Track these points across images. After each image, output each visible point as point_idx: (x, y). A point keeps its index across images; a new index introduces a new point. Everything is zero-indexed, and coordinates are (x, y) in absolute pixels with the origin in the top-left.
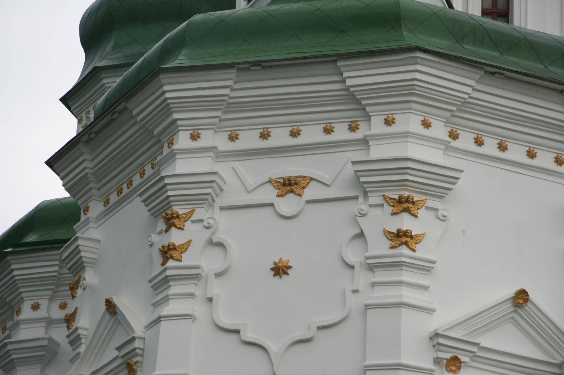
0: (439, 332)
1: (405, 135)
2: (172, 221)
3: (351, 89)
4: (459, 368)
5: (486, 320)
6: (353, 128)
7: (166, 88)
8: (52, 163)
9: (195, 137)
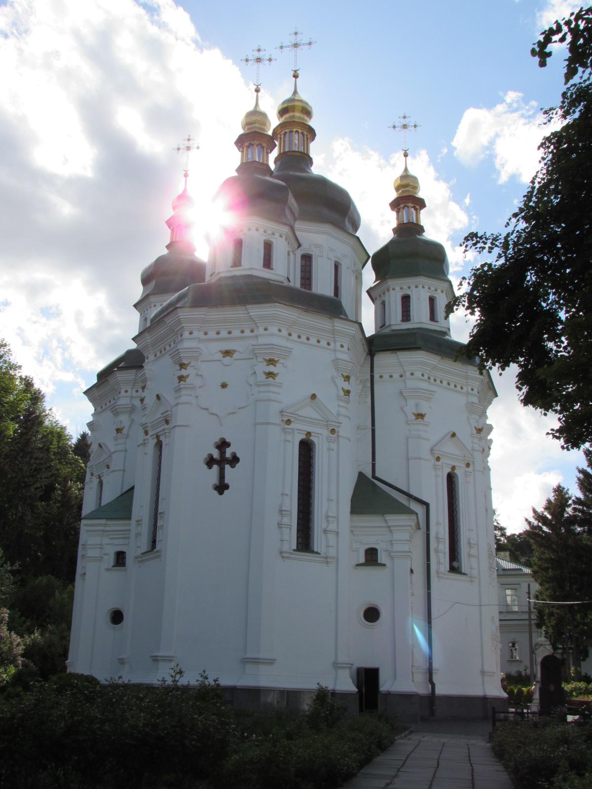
0: (284, 410)
1: (272, 335)
2: (182, 366)
3: (252, 317)
4: (290, 423)
6: (252, 331)
7: (179, 314)
8: (134, 339)
9: (191, 333)
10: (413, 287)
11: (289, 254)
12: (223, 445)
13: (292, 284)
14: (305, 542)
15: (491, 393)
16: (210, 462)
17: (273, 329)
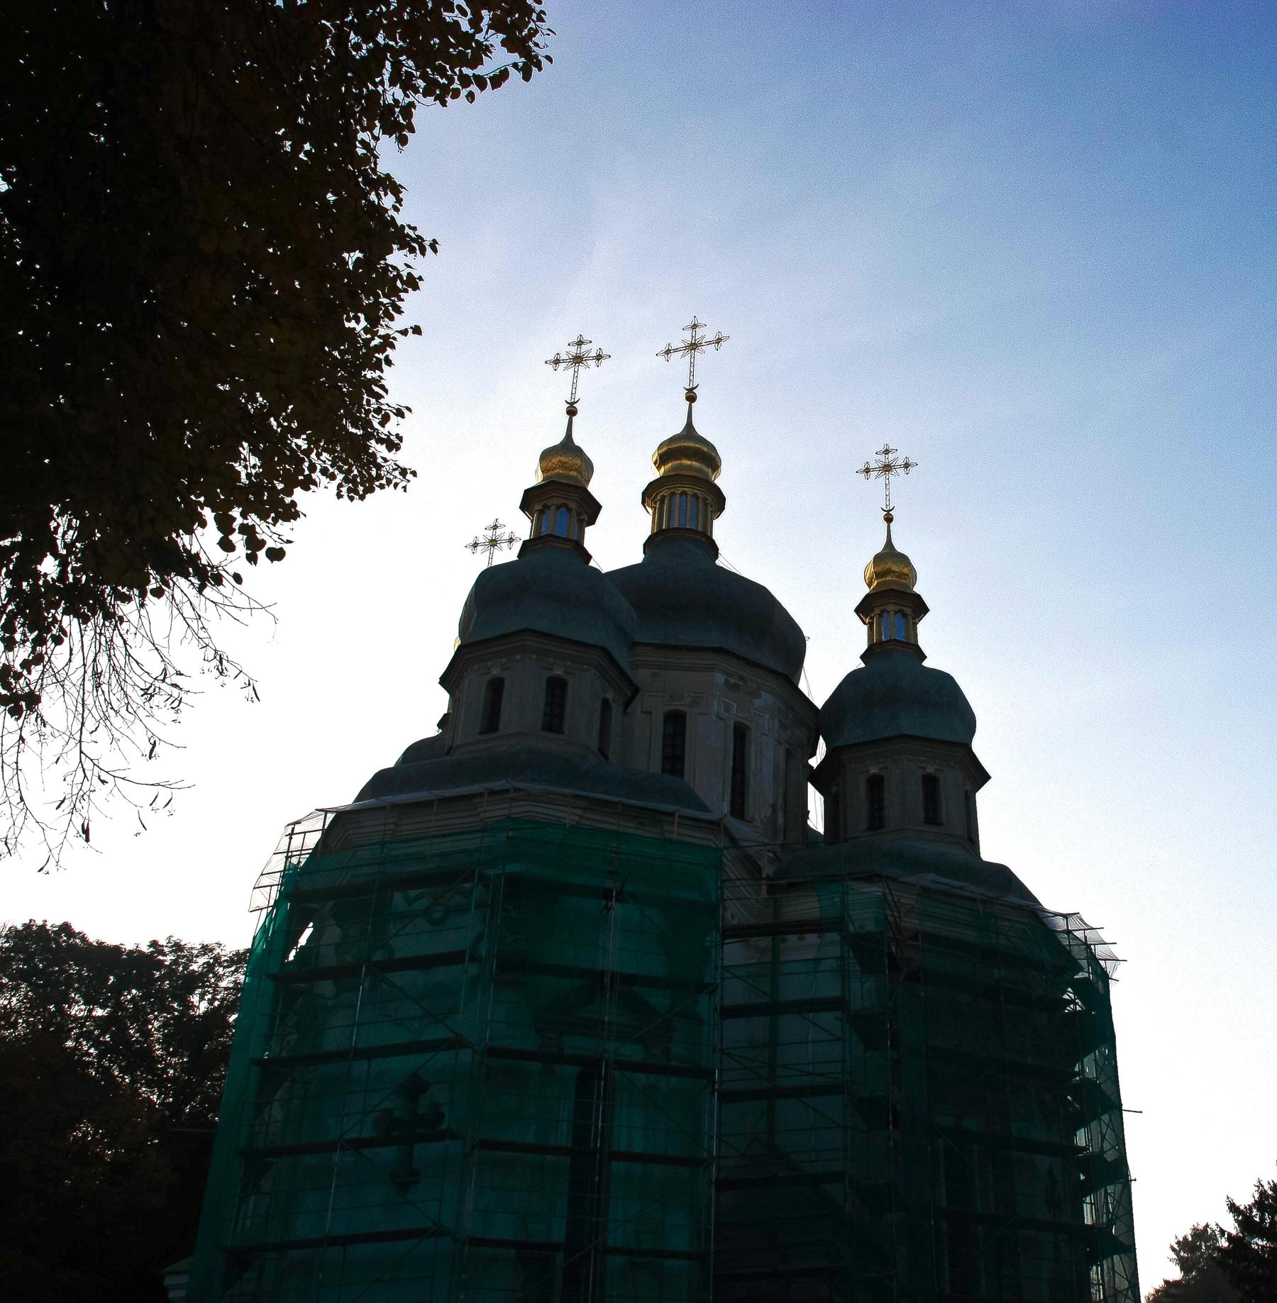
11: (606, 705)
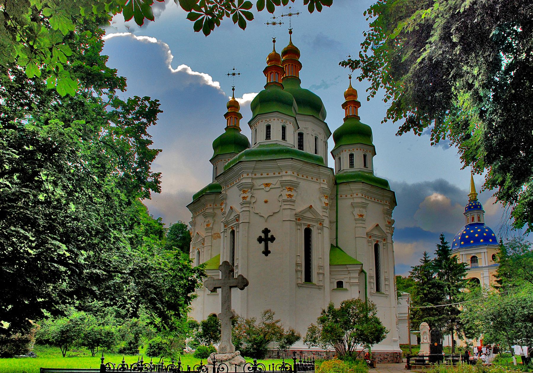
5: (305, 211)
10: (355, 150)
12: (266, 231)
13: (295, 149)
14: (308, 278)
15: (395, 204)
16: (260, 240)
17: (289, 173)
